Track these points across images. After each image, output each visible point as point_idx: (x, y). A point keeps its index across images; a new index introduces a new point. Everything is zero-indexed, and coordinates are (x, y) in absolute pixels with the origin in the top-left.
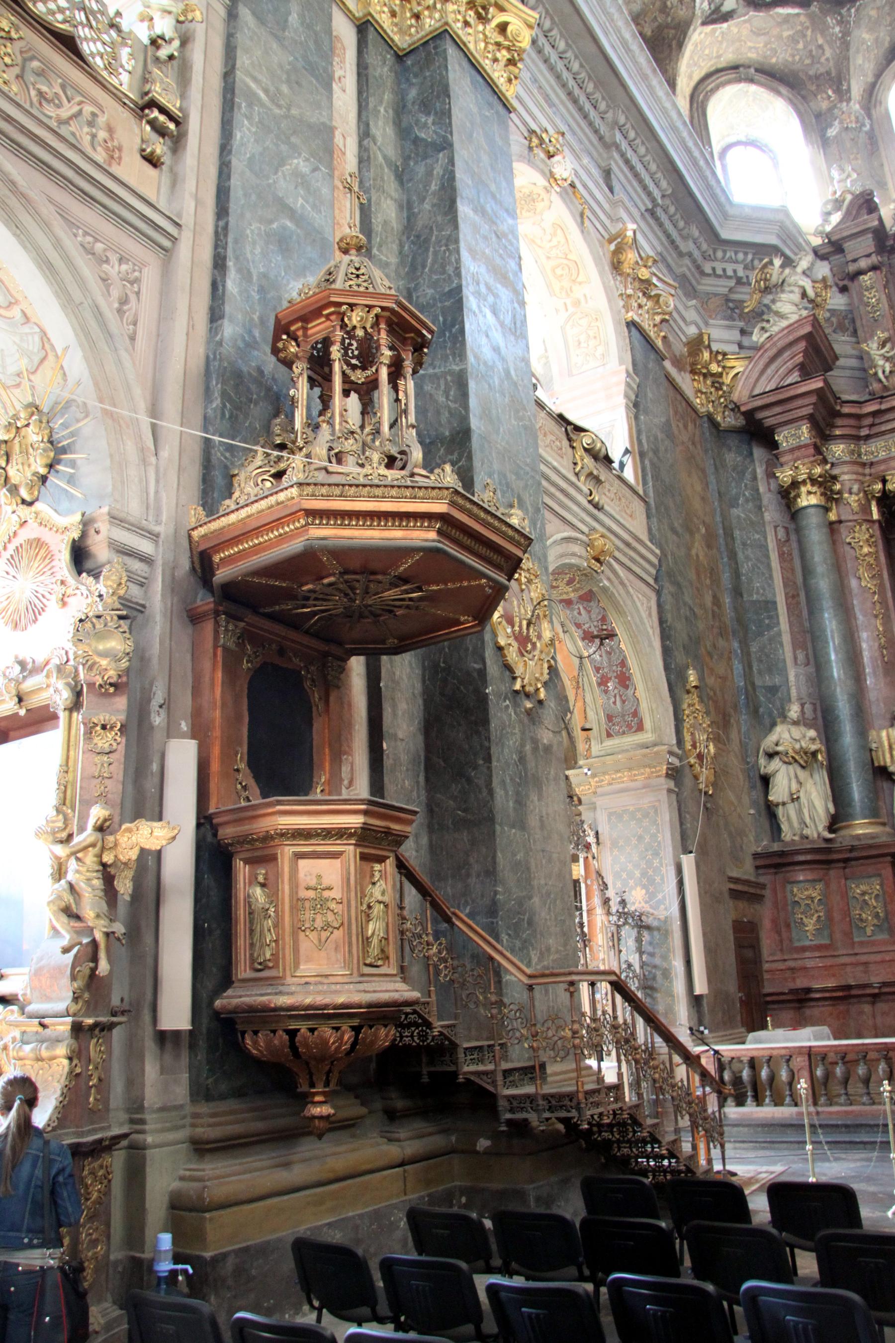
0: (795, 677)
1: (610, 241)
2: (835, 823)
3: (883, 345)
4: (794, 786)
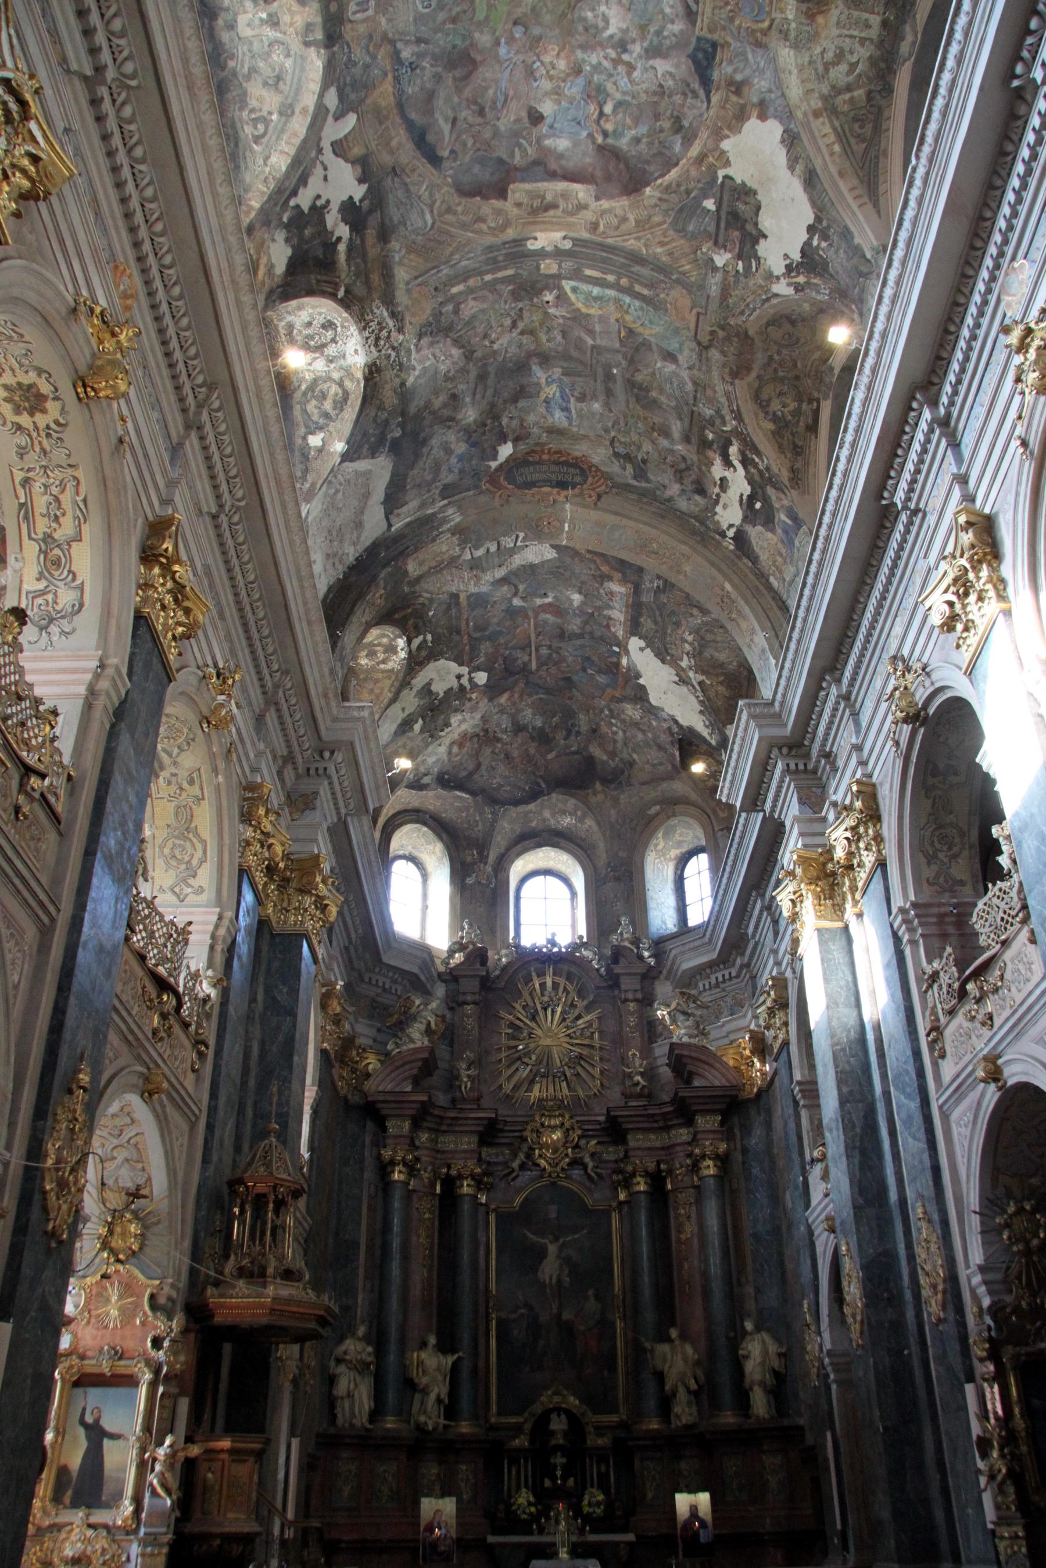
2: (375, 1415)
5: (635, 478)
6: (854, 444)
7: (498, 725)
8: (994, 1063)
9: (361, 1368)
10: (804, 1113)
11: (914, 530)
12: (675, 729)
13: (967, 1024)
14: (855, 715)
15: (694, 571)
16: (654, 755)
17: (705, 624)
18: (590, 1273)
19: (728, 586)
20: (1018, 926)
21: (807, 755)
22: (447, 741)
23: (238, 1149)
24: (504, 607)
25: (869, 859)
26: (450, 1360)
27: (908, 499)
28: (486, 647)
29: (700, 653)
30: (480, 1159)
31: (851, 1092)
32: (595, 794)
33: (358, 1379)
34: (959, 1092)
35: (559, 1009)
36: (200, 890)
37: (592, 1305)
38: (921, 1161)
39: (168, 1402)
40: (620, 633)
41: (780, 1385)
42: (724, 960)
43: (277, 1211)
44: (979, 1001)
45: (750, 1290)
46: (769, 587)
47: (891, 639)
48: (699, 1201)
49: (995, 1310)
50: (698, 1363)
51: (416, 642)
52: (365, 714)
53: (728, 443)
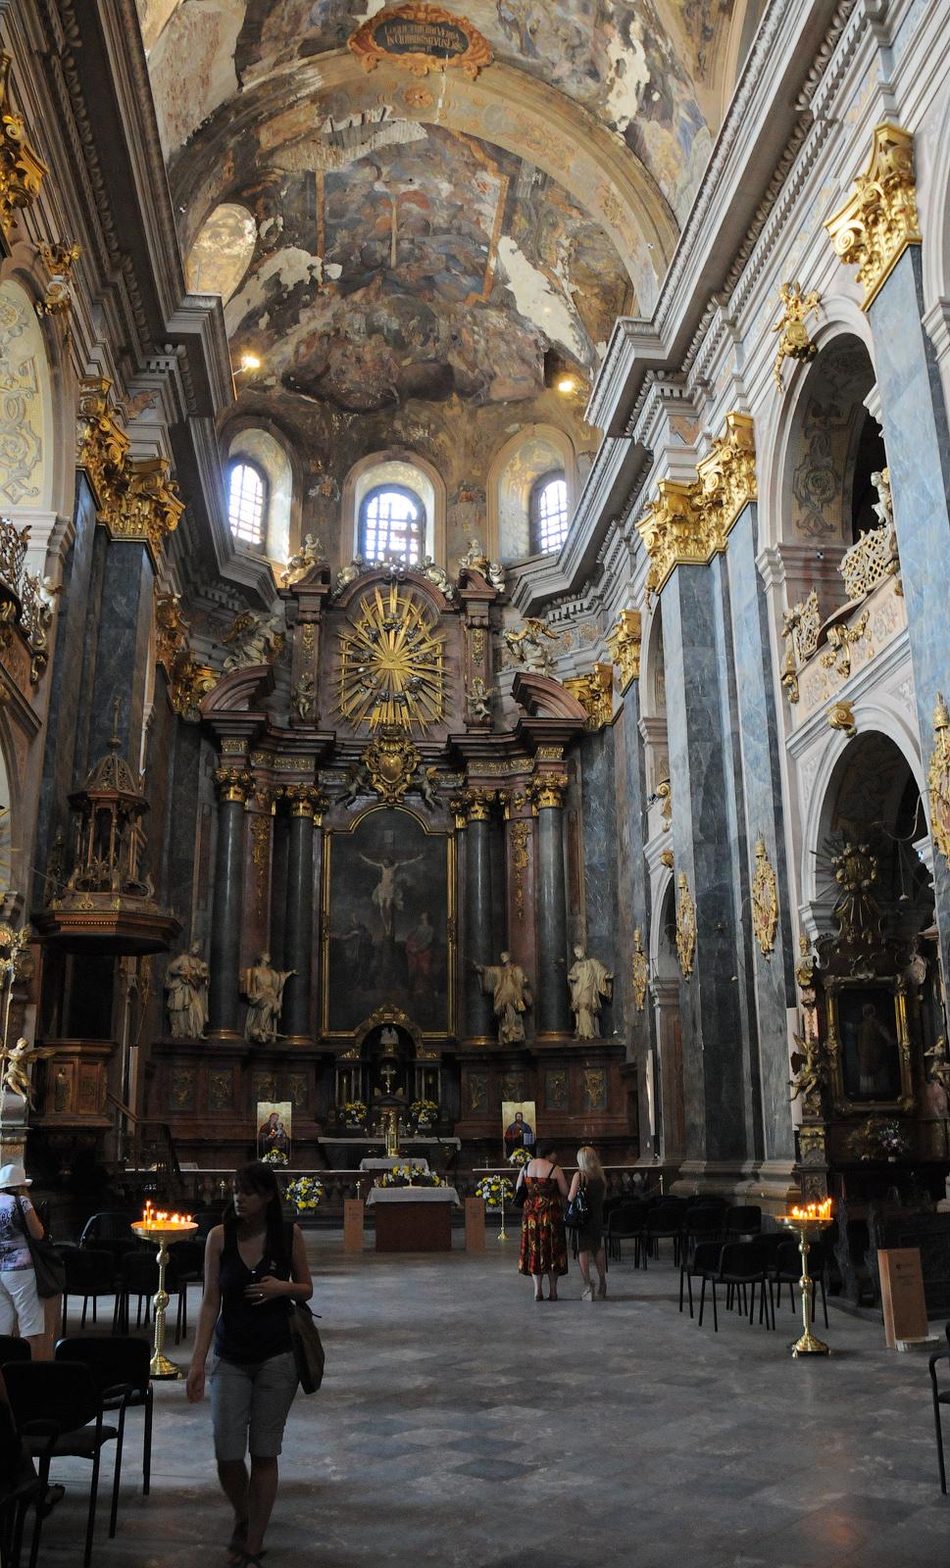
0: (198, 920)
1: (159, 599)
2: (209, 1028)
3: (307, 689)
4: (187, 1000)
5: (521, 50)
6: (775, 36)
7: (351, 325)
8: (847, 711)
9: (196, 983)
10: (649, 751)
11: (827, 143)
12: (542, 342)
13: (823, 671)
14: (739, 342)
15: (578, 169)
16: (516, 369)
17: (585, 228)
18: (424, 897)
19: (614, 188)
20: (885, 576)
21: (684, 382)
22: (294, 340)
23: (76, 765)
24: (364, 192)
25: (739, 497)
26: (284, 977)
27: (826, 107)
28: (342, 236)
29: (577, 260)
30: (316, 781)
31: (699, 731)
32: (451, 406)
33: (193, 993)
34: (809, 736)
35: (402, 633)
36: (36, 492)
37: (424, 928)
38: (765, 802)
39: (18, 1009)
40: (491, 232)
41: (605, 1010)
42: (576, 590)
43: (121, 826)
44: (838, 648)
45: (582, 919)
46: (659, 193)
47: (787, 264)
48: (537, 831)
49: (823, 945)
50: (526, 986)
51: (267, 225)
52: (213, 304)
53: (630, 17)
